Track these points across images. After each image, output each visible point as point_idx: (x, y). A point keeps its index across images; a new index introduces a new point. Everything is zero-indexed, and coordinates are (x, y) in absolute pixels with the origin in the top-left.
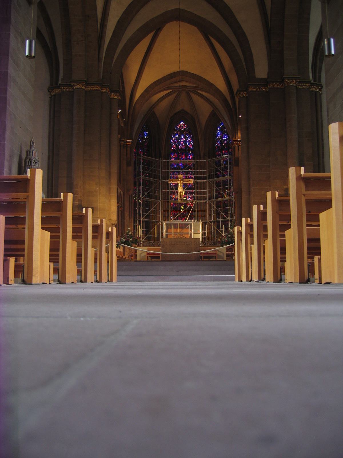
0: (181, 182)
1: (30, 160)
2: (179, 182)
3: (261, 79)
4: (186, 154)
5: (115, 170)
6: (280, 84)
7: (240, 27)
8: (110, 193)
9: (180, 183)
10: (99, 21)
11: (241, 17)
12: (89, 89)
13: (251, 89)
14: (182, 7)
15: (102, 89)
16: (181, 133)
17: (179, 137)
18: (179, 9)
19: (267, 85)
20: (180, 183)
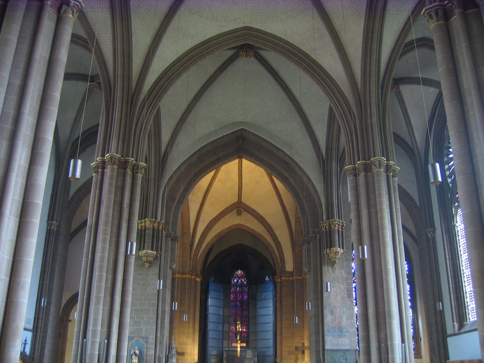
0: (239, 345)
1: (172, 348)
2: (238, 345)
3: (289, 272)
4: (242, 295)
5: (197, 327)
6: (300, 276)
7: (277, 238)
8: (194, 342)
9: (239, 346)
10: (191, 234)
11: (277, 232)
12: (184, 277)
13: (283, 278)
14: (242, 223)
15: (191, 276)
16: (239, 278)
17: (237, 281)
18: (240, 224)
19: (292, 276)
20: (239, 346)
